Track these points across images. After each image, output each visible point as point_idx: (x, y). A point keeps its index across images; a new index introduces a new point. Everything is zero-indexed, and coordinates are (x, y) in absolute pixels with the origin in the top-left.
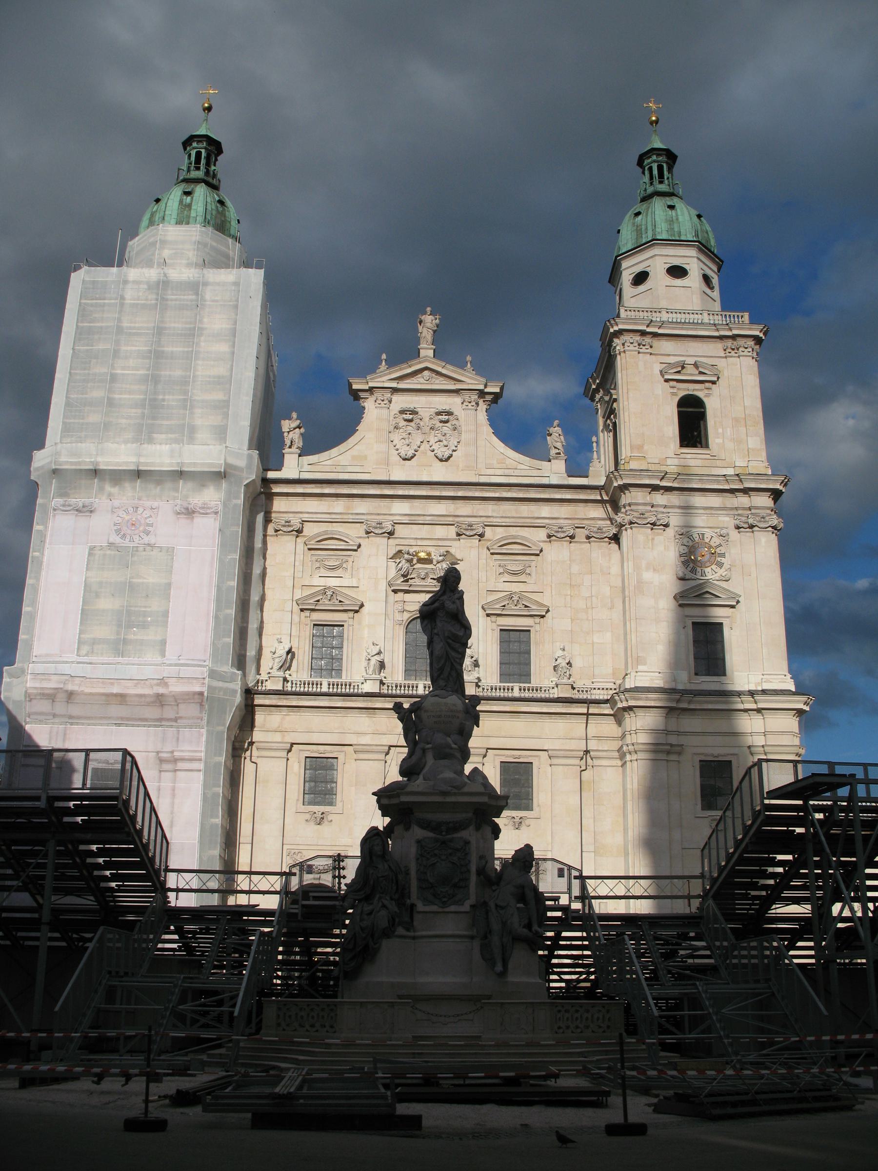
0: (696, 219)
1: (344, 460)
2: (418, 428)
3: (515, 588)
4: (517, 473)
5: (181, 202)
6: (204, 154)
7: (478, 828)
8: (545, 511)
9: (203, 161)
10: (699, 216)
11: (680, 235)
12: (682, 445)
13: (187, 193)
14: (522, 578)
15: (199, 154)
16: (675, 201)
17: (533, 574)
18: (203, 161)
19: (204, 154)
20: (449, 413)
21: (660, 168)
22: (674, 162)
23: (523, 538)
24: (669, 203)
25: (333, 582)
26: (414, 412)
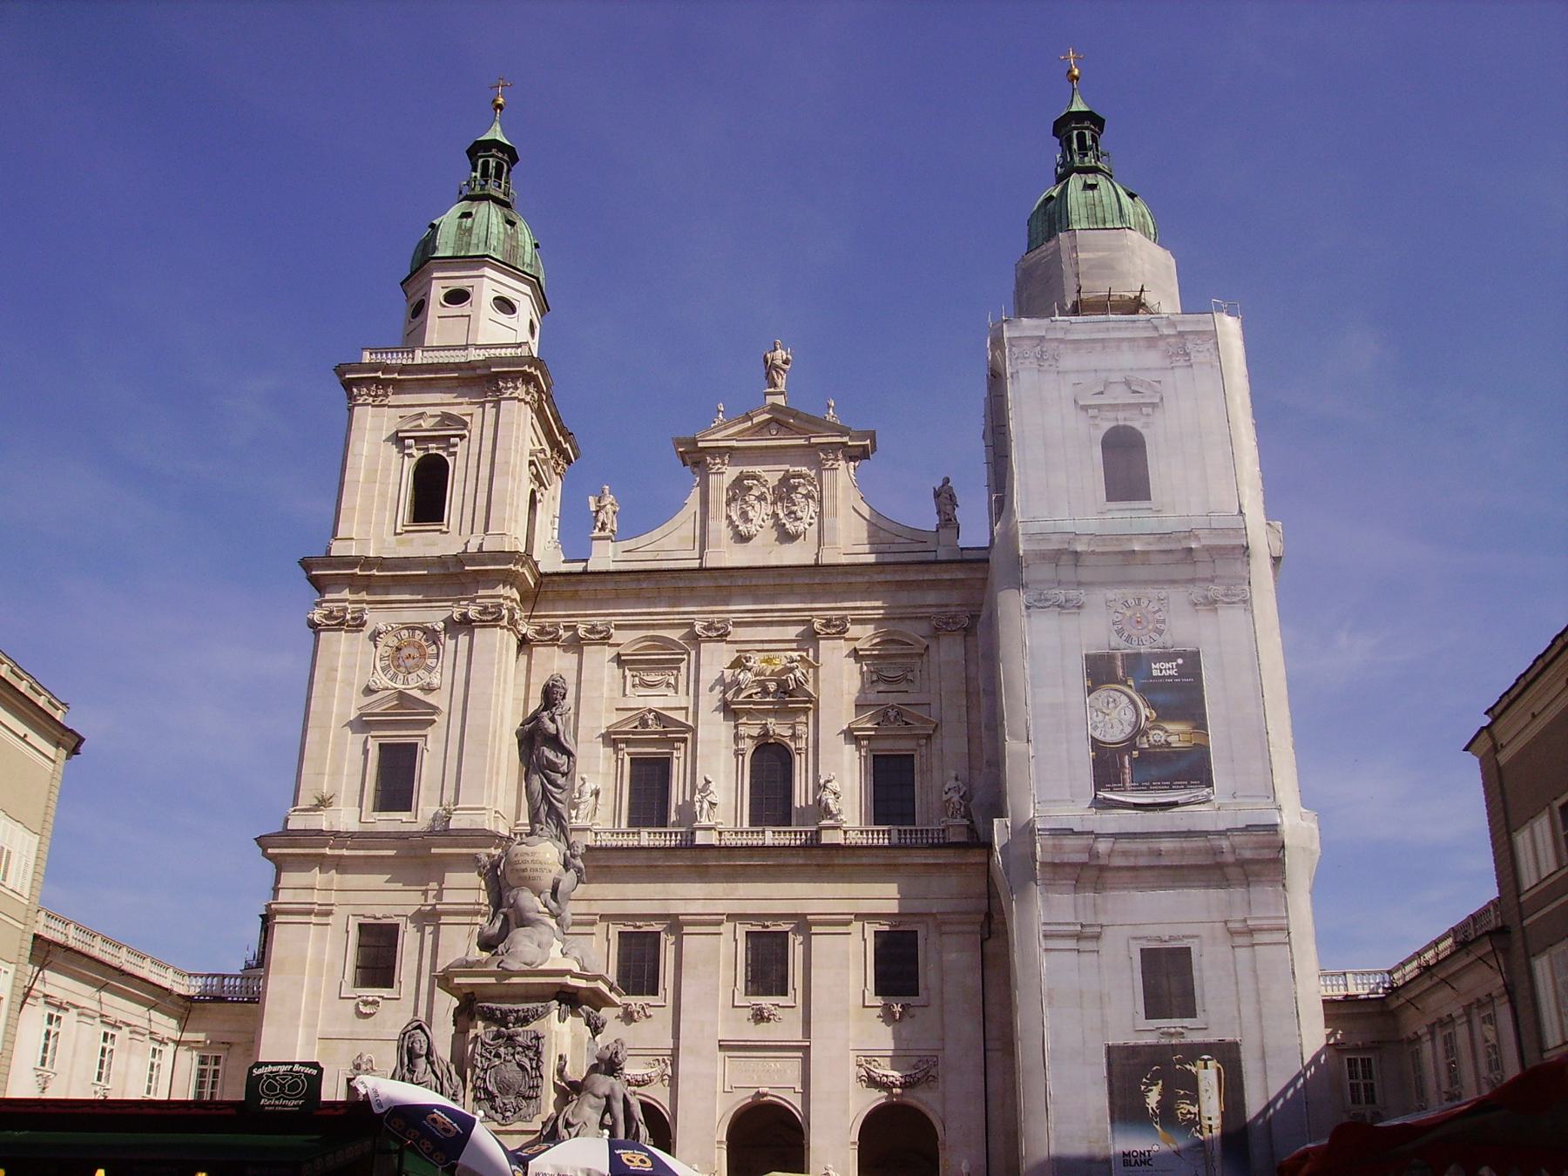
0: (1125, 199)
1: (668, 543)
2: (761, 498)
3: (892, 699)
4: (894, 548)
5: (460, 226)
6: (492, 163)
7: (562, 1019)
8: (931, 598)
9: (492, 171)
10: (1132, 196)
11: (1105, 223)
12: (1111, 497)
13: (467, 215)
14: (903, 686)
15: (486, 164)
16: (1100, 178)
17: (917, 682)
18: (492, 171)
19: (492, 163)
20: (800, 476)
21: (1081, 138)
22: (1102, 130)
23: (900, 633)
24: (1089, 182)
25: (656, 703)
26: (754, 477)
